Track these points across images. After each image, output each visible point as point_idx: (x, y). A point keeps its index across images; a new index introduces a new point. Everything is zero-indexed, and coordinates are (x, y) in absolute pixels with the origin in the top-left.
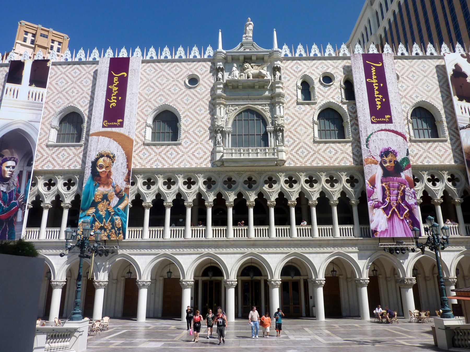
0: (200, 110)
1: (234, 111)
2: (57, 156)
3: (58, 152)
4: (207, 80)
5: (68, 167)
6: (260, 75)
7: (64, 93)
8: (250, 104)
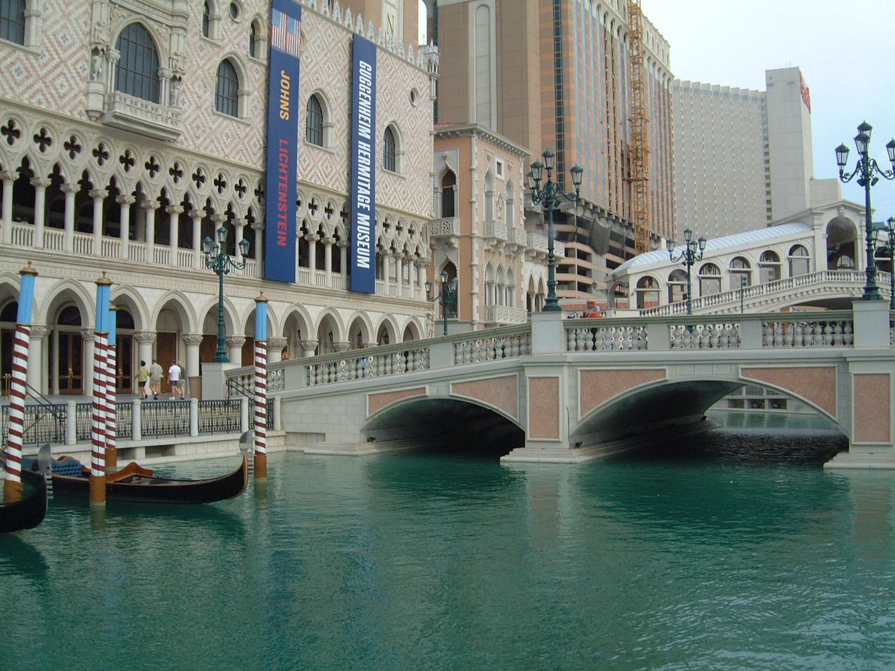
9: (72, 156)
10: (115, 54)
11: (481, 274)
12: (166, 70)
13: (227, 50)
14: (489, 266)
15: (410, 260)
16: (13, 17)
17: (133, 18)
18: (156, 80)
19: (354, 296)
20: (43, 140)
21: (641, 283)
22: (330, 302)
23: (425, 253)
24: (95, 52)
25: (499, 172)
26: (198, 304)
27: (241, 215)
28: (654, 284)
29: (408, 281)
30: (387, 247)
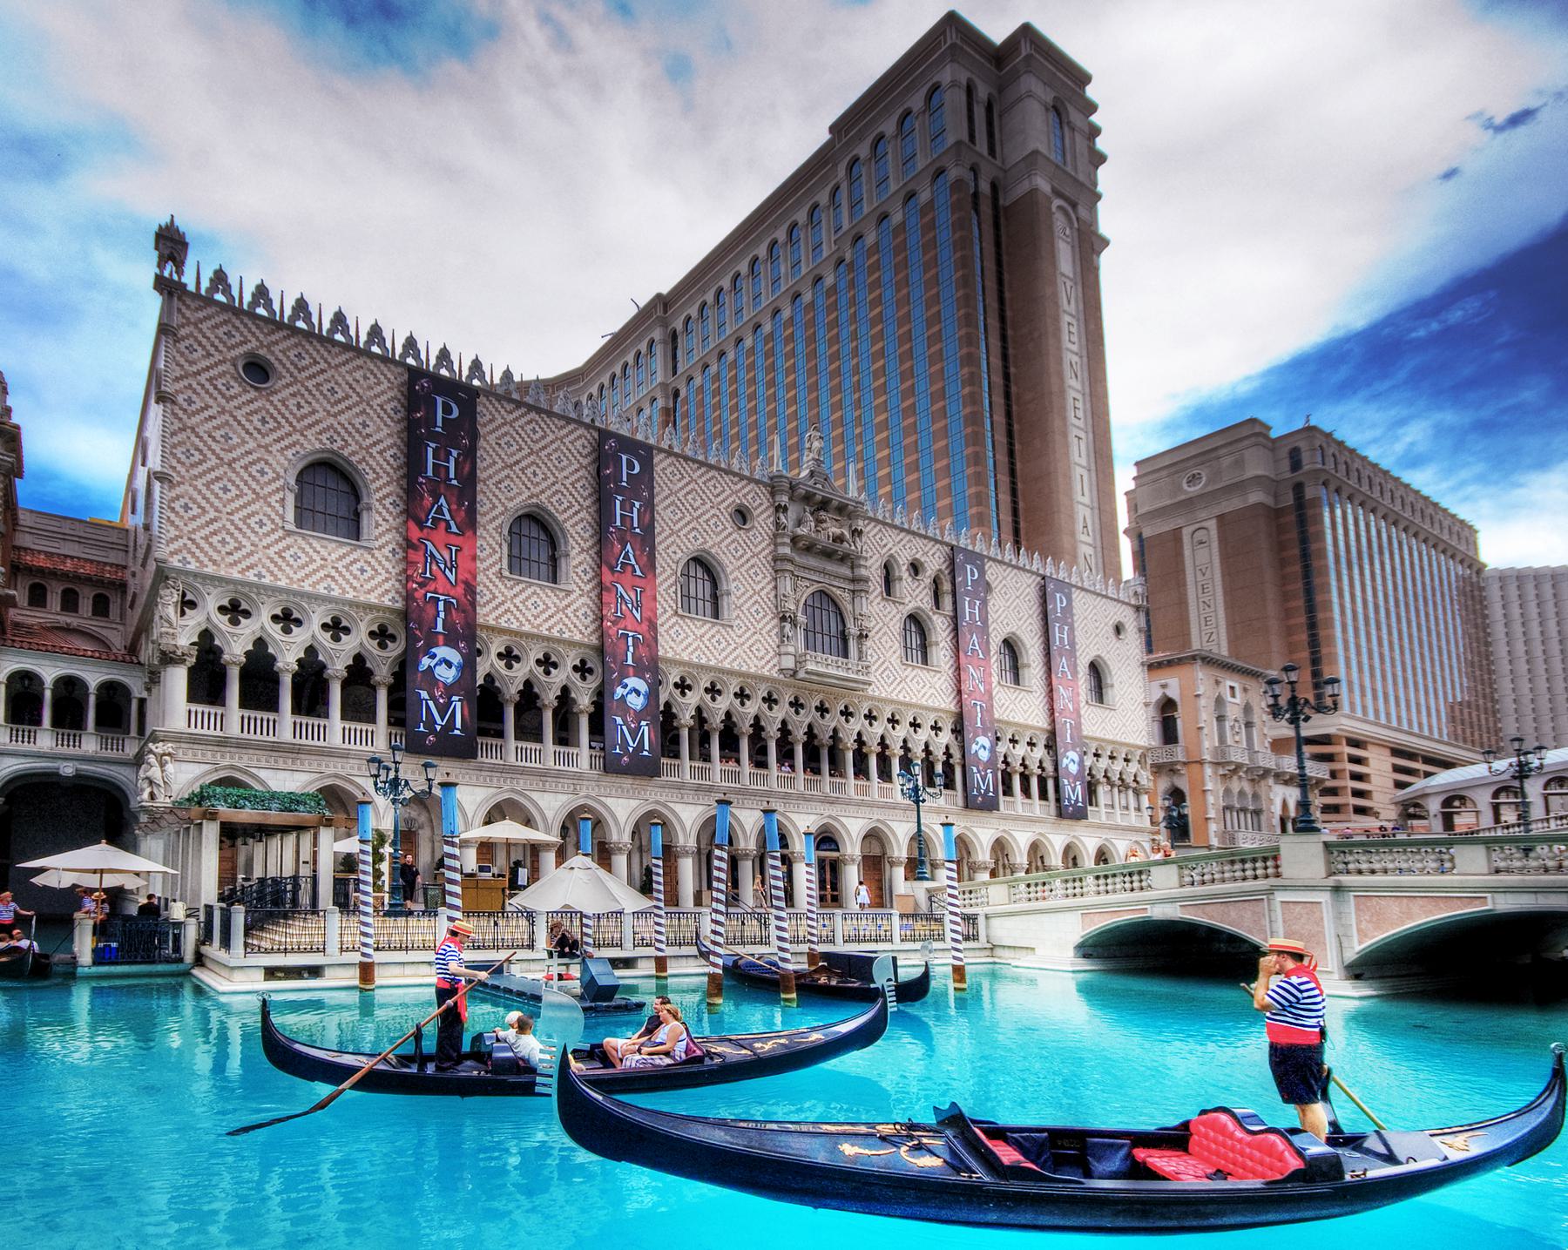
0: (756, 574)
1: (806, 591)
2: (523, 602)
3: (523, 596)
4: (763, 520)
5: (549, 629)
6: (839, 539)
7: (516, 468)
8: (826, 583)
9: (770, 708)
10: (801, 618)
11: (1217, 798)
12: (853, 630)
13: (911, 606)
14: (1227, 792)
15: (1127, 788)
16: (708, 597)
17: (816, 587)
18: (844, 638)
19: (1065, 822)
20: (742, 695)
21: (1447, 803)
22: (1038, 829)
23: (1145, 778)
24: (783, 619)
25: (1233, 696)
26: (900, 834)
27: (939, 754)
28: (1469, 803)
29: (1127, 808)
30: (1100, 776)
